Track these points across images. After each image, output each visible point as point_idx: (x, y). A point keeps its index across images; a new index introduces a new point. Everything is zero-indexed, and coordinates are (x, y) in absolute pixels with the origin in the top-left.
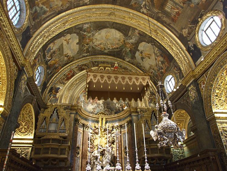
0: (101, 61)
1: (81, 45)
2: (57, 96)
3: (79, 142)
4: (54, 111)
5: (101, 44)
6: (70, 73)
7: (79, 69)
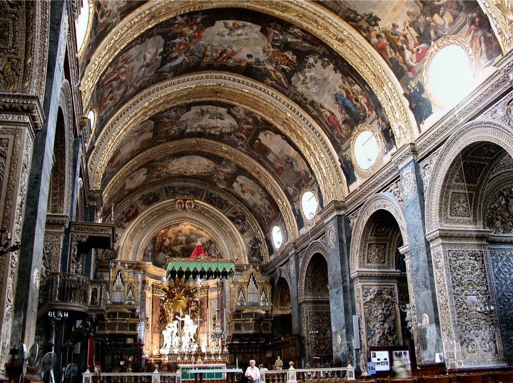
0: (179, 188)
1: (150, 174)
2: (116, 248)
3: (148, 311)
4: (116, 276)
5: (180, 168)
6: (132, 209)
7: (144, 202)
